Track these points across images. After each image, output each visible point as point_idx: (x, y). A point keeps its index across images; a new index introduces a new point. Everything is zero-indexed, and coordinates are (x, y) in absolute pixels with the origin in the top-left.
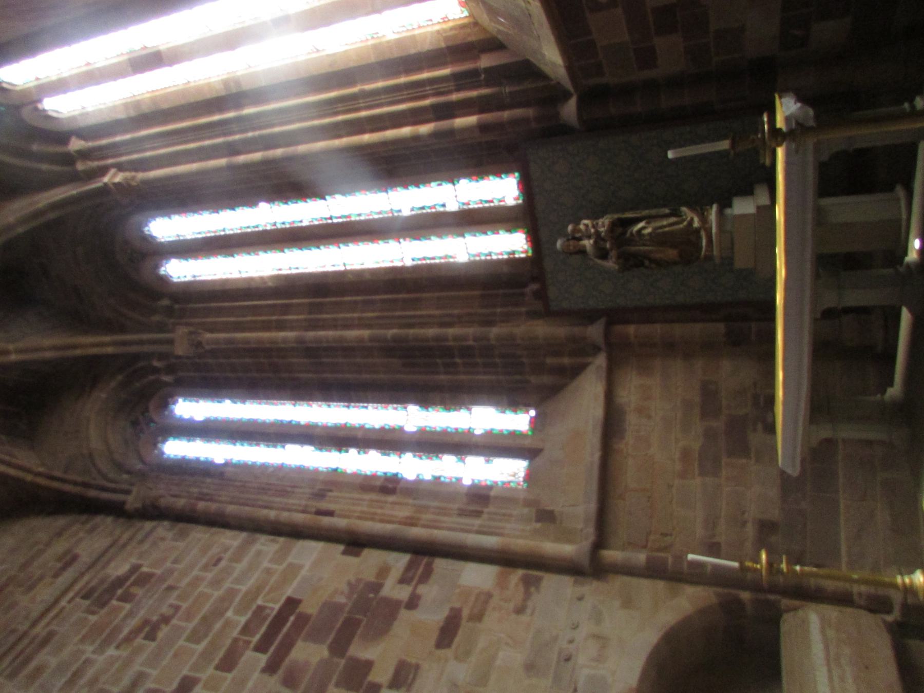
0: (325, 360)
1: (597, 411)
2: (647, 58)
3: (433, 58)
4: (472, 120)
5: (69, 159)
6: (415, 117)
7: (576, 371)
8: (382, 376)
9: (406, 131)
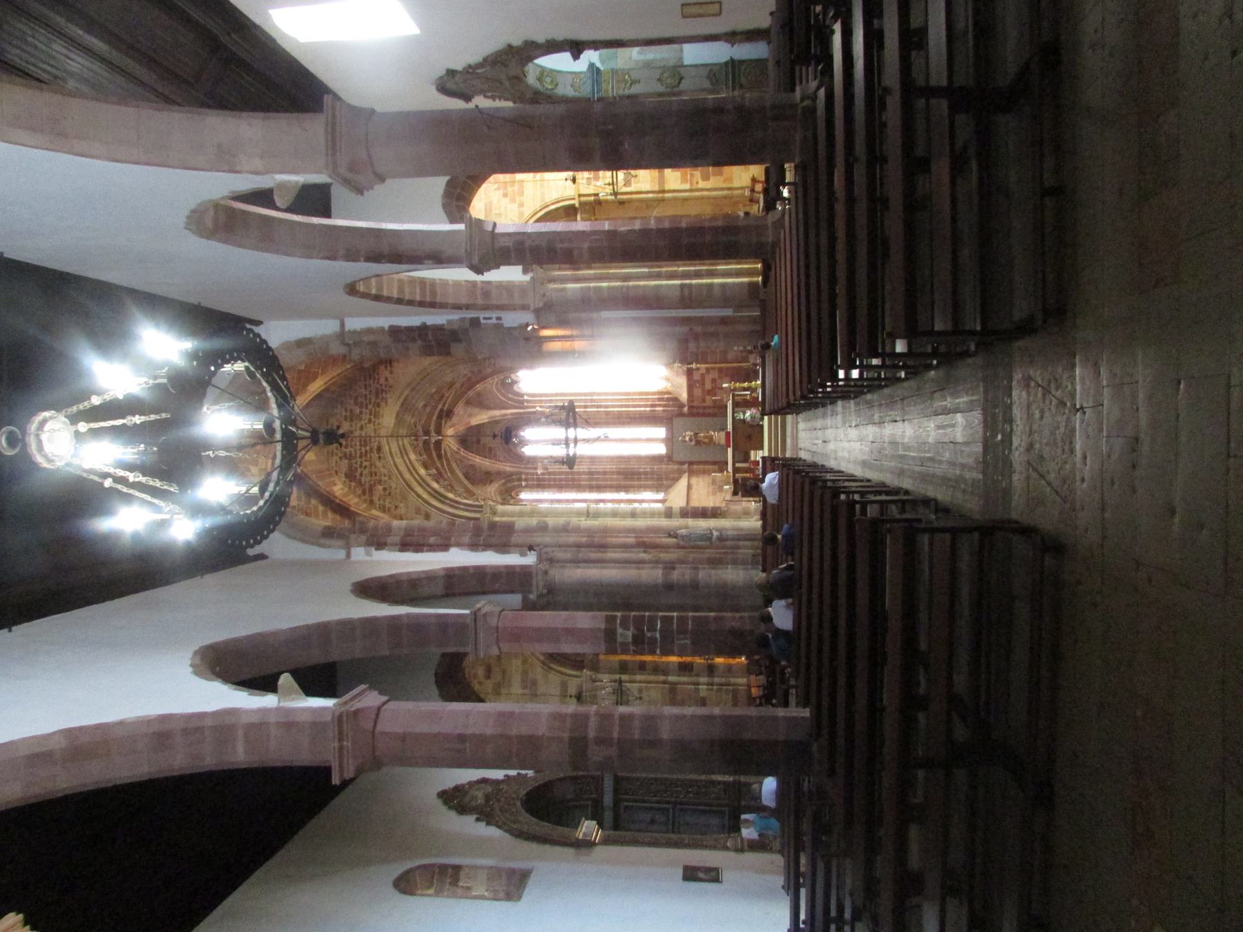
1: (686, 484)
2: (704, 401)
3: (654, 394)
4: (661, 409)
5: (522, 402)
6: (646, 406)
7: (677, 479)
9: (643, 409)
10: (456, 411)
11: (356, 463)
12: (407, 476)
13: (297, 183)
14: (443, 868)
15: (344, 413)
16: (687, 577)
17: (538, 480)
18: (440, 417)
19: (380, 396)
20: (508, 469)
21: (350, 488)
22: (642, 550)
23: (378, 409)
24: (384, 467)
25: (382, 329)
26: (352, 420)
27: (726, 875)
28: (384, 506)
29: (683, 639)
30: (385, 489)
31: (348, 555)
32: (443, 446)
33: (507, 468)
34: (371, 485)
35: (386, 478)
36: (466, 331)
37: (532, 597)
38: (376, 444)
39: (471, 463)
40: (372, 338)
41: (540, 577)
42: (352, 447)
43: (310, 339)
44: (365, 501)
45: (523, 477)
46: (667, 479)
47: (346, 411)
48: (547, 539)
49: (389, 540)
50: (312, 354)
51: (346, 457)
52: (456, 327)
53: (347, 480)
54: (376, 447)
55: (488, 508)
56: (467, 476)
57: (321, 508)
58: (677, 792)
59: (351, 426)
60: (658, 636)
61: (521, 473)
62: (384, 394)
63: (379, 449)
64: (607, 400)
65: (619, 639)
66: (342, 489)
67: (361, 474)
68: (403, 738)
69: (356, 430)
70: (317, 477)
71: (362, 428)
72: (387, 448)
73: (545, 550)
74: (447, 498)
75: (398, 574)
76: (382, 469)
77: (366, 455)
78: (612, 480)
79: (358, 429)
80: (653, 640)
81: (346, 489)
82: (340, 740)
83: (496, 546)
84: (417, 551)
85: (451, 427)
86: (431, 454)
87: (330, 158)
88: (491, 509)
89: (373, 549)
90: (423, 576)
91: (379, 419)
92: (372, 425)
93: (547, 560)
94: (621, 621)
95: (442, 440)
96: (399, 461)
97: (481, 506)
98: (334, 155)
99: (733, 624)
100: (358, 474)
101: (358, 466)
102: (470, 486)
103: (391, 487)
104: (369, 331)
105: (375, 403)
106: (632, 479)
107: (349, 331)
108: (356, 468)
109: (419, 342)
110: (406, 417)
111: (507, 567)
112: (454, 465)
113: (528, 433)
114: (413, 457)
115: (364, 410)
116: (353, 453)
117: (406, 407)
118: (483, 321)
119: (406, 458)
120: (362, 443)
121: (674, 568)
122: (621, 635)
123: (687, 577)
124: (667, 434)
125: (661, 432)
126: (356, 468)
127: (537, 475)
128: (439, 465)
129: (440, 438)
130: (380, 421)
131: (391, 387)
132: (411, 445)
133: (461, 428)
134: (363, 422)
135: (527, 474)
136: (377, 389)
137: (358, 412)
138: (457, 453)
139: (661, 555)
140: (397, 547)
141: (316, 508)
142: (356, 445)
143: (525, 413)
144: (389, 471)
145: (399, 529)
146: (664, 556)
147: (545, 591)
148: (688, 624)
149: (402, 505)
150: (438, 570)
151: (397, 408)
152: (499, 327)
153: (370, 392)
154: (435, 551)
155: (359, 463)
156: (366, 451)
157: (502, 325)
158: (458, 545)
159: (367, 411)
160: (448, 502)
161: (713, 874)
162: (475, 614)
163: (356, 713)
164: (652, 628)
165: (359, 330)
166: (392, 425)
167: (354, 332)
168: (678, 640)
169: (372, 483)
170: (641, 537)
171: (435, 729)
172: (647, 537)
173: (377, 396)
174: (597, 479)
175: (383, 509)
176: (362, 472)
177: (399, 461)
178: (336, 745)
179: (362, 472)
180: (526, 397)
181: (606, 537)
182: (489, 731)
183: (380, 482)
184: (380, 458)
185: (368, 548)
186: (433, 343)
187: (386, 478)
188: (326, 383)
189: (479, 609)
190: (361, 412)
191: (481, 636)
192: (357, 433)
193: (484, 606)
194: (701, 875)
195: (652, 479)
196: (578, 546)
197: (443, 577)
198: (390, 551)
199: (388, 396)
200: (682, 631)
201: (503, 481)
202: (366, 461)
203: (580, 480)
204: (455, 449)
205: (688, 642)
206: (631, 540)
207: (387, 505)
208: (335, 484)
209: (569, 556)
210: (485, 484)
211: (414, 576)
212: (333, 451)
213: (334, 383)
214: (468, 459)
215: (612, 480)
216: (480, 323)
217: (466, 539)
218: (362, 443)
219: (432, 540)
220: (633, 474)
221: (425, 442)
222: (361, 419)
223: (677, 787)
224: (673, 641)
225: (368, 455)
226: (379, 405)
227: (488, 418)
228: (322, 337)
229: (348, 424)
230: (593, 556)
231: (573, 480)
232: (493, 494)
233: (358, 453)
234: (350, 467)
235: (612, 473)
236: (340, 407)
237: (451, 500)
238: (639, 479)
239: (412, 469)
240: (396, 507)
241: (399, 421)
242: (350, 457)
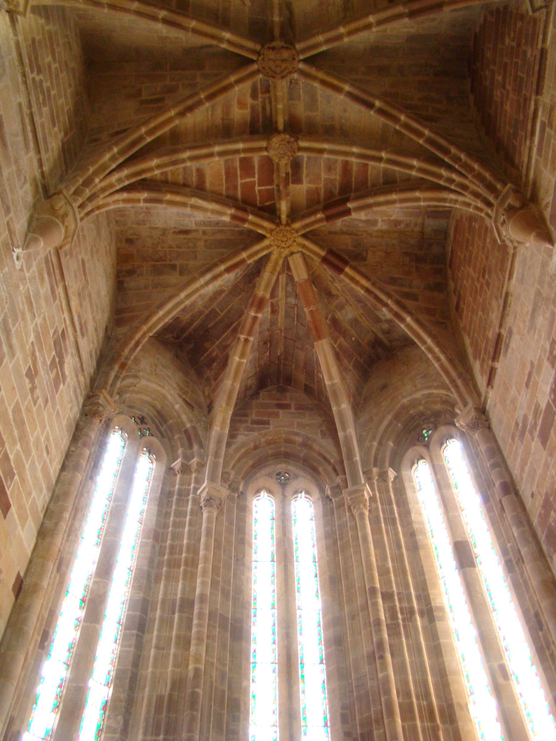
0: (176, 616)
64: (416, 650)
78: (160, 660)
95: (279, 224)
129: (284, 217)
135: (201, 466)
174: (166, 622)
180: (392, 474)
201: (188, 425)
231: (174, 564)
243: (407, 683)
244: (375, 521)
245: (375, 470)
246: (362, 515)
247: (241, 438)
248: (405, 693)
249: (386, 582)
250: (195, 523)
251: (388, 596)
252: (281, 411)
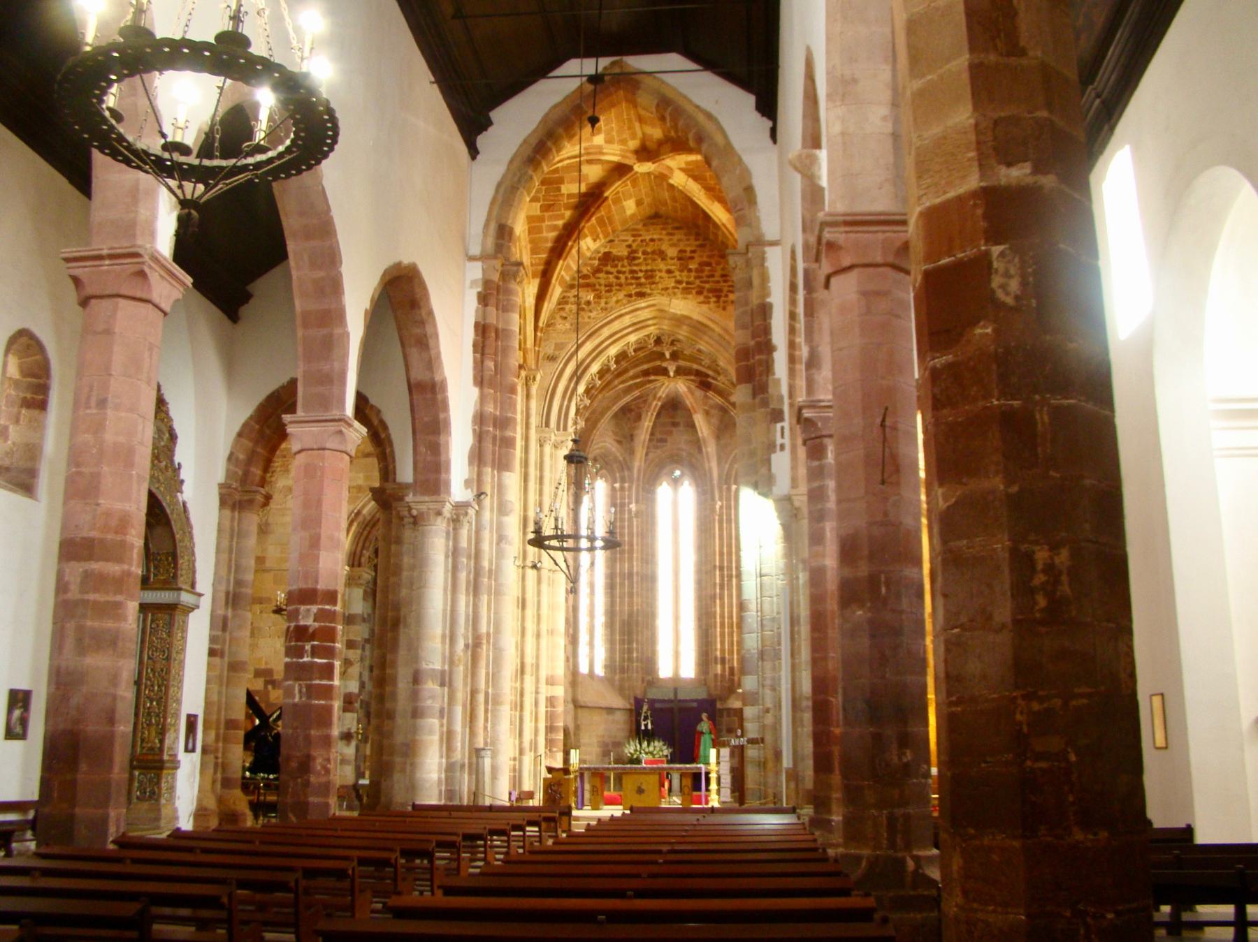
1: (614, 706)
6: (723, 650)
8: (618, 608)
9: (719, 646)
10: (710, 394)
11: (623, 266)
12: (606, 332)
13: (819, 178)
14: (43, 389)
15: (688, 249)
16: (429, 702)
17: (623, 505)
18: (698, 373)
19: (711, 295)
20: (636, 464)
21: (591, 259)
22: (470, 641)
23: (694, 291)
24: (617, 302)
25: (768, 295)
26: (680, 259)
27: (17, 745)
28: (567, 303)
29: (300, 692)
30: (588, 303)
31: (472, 259)
32: (661, 378)
33: (638, 462)
34: (595, 285)
35: (603, 305)
36: (765, 403)
37: (410, 498)
38: (648, 291)
39: (643, 416)
40: (756, 281)
41: (432, 506)
42: (645, 259)
43: (755, 203)
44: (573, 279)
45: (626, 485)
46: (622, 680)
47: (693, 252)
48: (487, 515)
49: (492, 310)
50: (736, 206)
51: (630, 253)
52: (771, 390)
53: (600, 255)
54: (644, 290)
55: (564, 439)
56: (625, 410)
57: (560, 223)
58: (153, 686)
59: (672, 259)
60: (305, 659)
61: (631, 482)
62: (713, 299)
63: (641, 295)
64: (730, 596)
65: (303, 608)
66: (588, 249)
67: (608, 273)
68: (108, 332)
69: (667, 265)
70: (602, 216)
71: (669, 272)
72: (643, 305)
73: (471, 512)
74: (577, 383)
75: (434, 319)
76: (614, 299)
77: (633, 278)
78: (622, 603)
79: (669, 267)
80: (299, 652)
81: (588, 254)
82: (111, 257)
83: (480, 448)
84: (475, 345)
85: (689, 388)
86: (649, 362)
87: (841, 218)
88: (562, 442)
89: (479, 289)
90: (433, 352)
91: (682, 293)
92: (673, 284)
93: (458, 515)
94: (329, 611)
95: (669, 376)
96: (627, 320)
97: (565, 429)
98: (846, 223)
99: (319, 761)
100: (609, 268)
101: (619, 268)
102: (610, 414)
103: (591, 311)
104: (765, 278)
105: (703, 288)
106: (622, 633)
107: (764, 253)
108: (616, 266)
109: (752, 343)
110: (685, 327)
111: (448, 463)
112: (636, 393)
113: (687, 492)
114: (633, 338)
115: (693, 274)
116: (637, 262)
117: (699, 328)
118: (779, 426)
119: (630, 329)
120: (650, 273)
121: (442, 685)
122: (308, 610)
123: (429, 702)
124: (685, 680)
125: (689, 670)
126: (616, 266)
127: (630, 503)
128: (631, 373)
129: (672, 374)
130: (679, 296)
131: (724, 309)
132: (648, 336)
133: (689, 401)
134: (677, 273)
135: (630, 488)
136: (721, 291)
137: (691, 267)
138: (655, 397)
139: (461, 668)
140: (480, 320)
141: (562, 217)
142: (647, 265)
143: (712, 486)
144: (612, 308)
145: (507, 322)
146: (460, 671)
147: (414, 512)
148: (319, 699)
149: (568, 326)
150: (442, 373)
151: (696, 316)
152: (771, 447)
153: (718, 282)
154: (475, 368)
155: (624, 269)
156: (638, 278)
157: (775, 452)
158: (482, 399)
159: (692, 279)
160: (572, 385)
161: (18, 730)
162: (341, 420)
163: (142, 274)
164: (315, 652)
165: (766, 264)
166: (672, 311)
167: (763, 259)
168: (300, 685)
169: (597, 287)
170: (488, 642)
171: (117, 368)
172: (488, 650)
173: (710, 291)
174: (622, 585)
175: (563, 301)
176: (612, 273)
177: (627, 320)
178: (105, 252)
179: (612, 273)
180: (734, 487)
181: (489, 595)
182: (109, 437)
183: (598, 297)
184: (630, 296)
185: (480, 283)
186: (752, 361)
187: (603, 305)
188: (724, 225)
189: (350, 425)
190: (690, 270)
191: (315, 429)
192: (662, 266)
193: (357, 431)
194: (17, 713)
195: (623, 660)
196: (478, 556)
197: (433, 379)
198: (477, 311)
199: (712, 305)
200: (311, 691)
201: (621, 459)
202: (626, 278)
203: (622, 560)
204: (660, 394)
205: (297, 700)
206: (483, 629)
207: (568, 307)
208: (595, 240)
209: (464, 543)
210: (615, 433)
211: (431, 343)
212: (640, 235)
213: (726, 237)
214: (647, 411)
215: (622, 603)
216: (776, 422)
217: (490, 408)
218: (650, 273)
219: (490, 364)
220: (630, 633)
221: (661, 356)
222: (681, 271)
223: (159, 686)
224: (297, 679)
225: (633, 281)
226: (699, 293)
227: (703, 436)
228: (758, 219)
229: (675, 255)
230: (463, 576)
232: (601, 444)
233: (635, 268)
234: (620, 259)
235: (631, 604)
236: (698, 243)
237: (575, 389)
238: (622, 642)
239: (614, 337)
240: (565, 318)
241: (680, 320)
242: (632, 257)
243: (724, 614)
244: (721, 522)
245: (725, 487)
246: (714, 519)
247: (651, 455)
248: (722, 616)
249: (721, 561)
250: (630, 526)
251: (721, 568)
252: (674, 429)
